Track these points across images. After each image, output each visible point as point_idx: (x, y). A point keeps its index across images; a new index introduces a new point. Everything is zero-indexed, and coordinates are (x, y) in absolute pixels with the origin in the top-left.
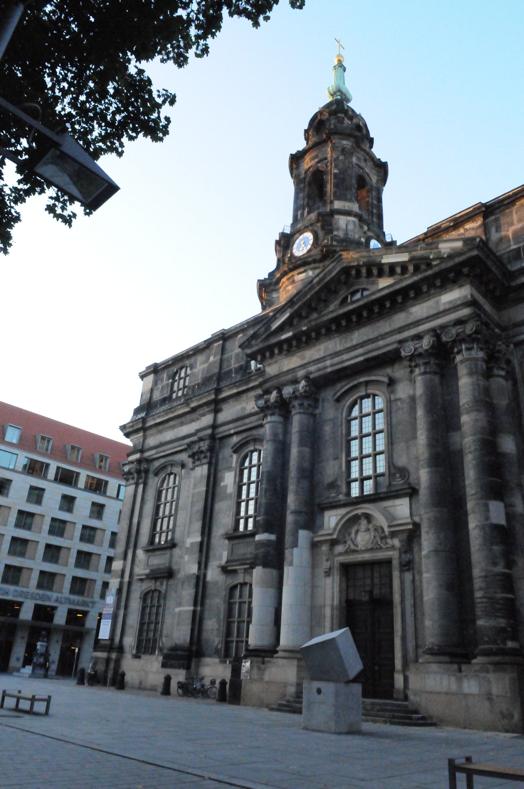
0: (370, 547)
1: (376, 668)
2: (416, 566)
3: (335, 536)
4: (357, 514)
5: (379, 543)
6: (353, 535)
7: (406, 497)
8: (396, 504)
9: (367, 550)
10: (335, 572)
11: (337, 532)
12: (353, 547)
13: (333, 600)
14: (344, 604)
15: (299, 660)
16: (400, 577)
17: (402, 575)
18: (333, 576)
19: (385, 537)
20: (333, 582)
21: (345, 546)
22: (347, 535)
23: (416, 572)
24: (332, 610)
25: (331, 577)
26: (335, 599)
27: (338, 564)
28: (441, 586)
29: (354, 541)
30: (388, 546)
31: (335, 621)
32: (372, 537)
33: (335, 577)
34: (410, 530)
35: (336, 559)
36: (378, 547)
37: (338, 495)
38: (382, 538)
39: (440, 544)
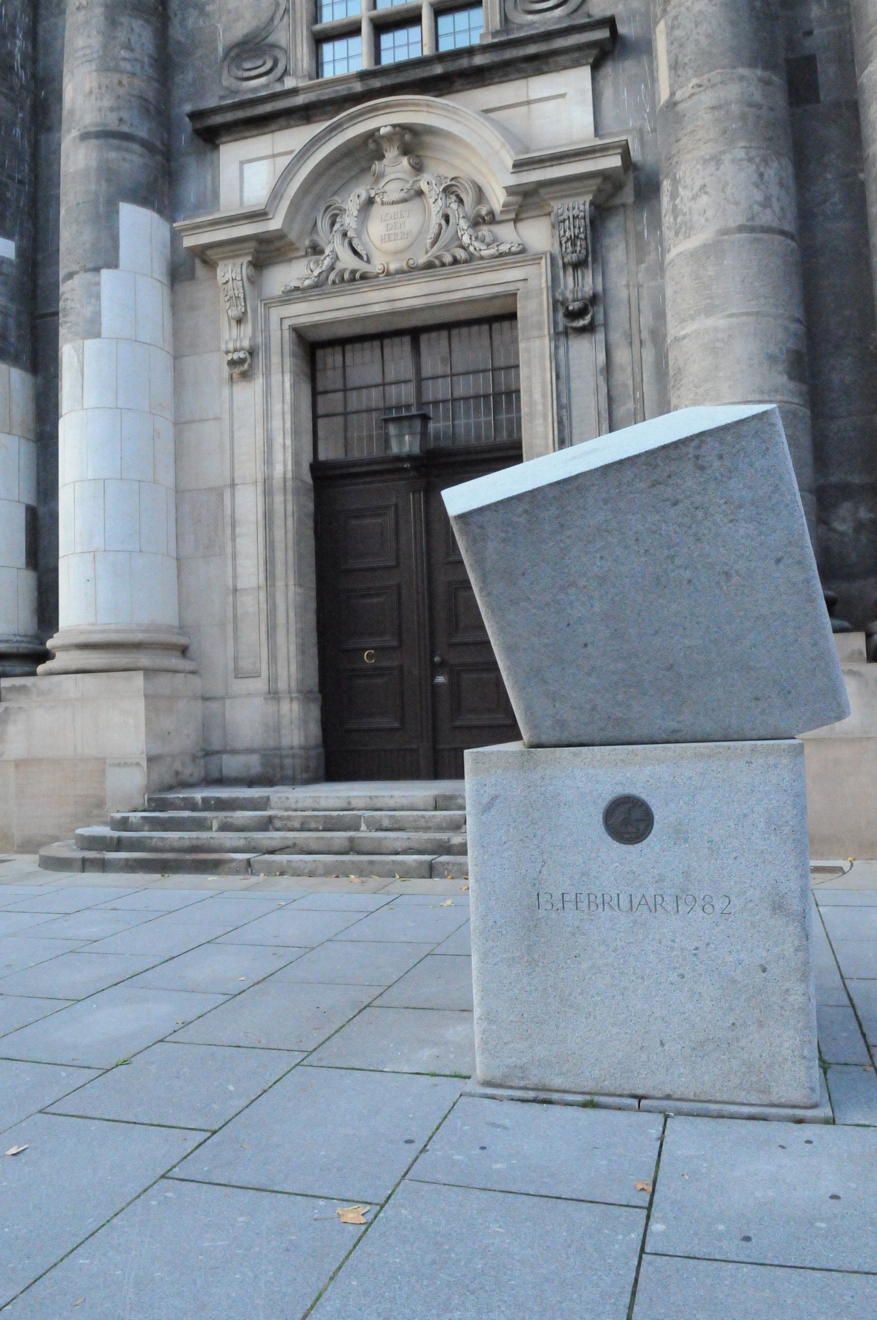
0: (422, 260)
1: (440, 679)
2: (619, 317)
3: (275, 224)
4: (372, 135)
5: (466, 240)
6: (349, 221)
7: (577, 64)
8: (533, 97)
9: (411, 271)
10: (275, 359)
11: (285, 204)
12: (348, 261)
13: (269, 461)
14: (308, 478)
15: (149, 672)
16: (555, 357)
17: (562, 351)
18: (267, 374)
19: (491, 219)
20: (267, 393)
21: (317, 262)
22: (323, 224)
23: (616, 336)
24: (268, 493)
25: (259, 382)
26: (278, 456)
27: (287, 334)
28: (772, 359)
29: (355, 243)
30: (504, 248)
31: (279, 534)
32: (436, 220)
33: (276, 378)
34: (604, 175)
35: (276, 314)
36: (461, 254)
37: (280, 79)
38: (477, 222)
39: (766, 204)
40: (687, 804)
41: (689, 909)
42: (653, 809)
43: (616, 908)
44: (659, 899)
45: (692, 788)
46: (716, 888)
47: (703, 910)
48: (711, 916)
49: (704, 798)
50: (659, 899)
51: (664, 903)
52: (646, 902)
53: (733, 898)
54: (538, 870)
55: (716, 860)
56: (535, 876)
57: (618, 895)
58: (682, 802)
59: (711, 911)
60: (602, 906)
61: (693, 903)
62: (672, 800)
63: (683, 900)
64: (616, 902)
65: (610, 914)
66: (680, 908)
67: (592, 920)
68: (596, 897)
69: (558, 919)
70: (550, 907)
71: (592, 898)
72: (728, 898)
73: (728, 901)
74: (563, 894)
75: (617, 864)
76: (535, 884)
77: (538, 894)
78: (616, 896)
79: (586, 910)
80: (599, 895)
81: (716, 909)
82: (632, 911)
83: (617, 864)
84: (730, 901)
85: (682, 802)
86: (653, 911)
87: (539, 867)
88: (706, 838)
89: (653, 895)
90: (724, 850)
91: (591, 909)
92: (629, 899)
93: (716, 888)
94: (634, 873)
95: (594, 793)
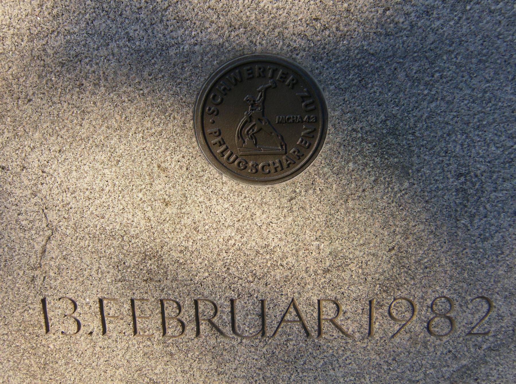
40: (415, 81)
41: (397, 327)
42: (326, 95)
43: (228, 330)
44: (329, 310)
45: (432, 37)
46: (464, 280)
47: (428, 328)
48: (445, 339)
49: (458, 66)
50: (329, 310)
51: (341, 317)
52: (298, 315)
53: (498, 301)
54: (38, 248)
55: (472, 217)
56: (32, 261)
57: (232, 301)
58: (401, 76)
59: (446, 331)
60: (193, 325)
61: (408, 315)
62: (377, 70)
63: (386, 308)
64: (227, 318)
65: (213, 341)
66: (376, 326)
67: (171, 354)
68: (179, 307)
69: (94, 354)
70: (75, 327)
71: (170, 310)
72: (489, 302)
73: (486, 306)
74: (101, 301)
75: (229, 232)
76: (33, 279)
77: (44, 301)
78: (229, 303)
79: (158, 335)
80: (187, 303)
81: (457, 325)
82: (263, 334)
83: (229, 232)
84: (490, 306)
85: (401, 76)
86: (314, 334)
87: (41, 240)
88: (453, 167)
89: (315, 299)
90: (493, 195)
91: (169, 332)
92: (258, 309)
93: (464, 280)
94: (273, 252)
95: (172, 52)
